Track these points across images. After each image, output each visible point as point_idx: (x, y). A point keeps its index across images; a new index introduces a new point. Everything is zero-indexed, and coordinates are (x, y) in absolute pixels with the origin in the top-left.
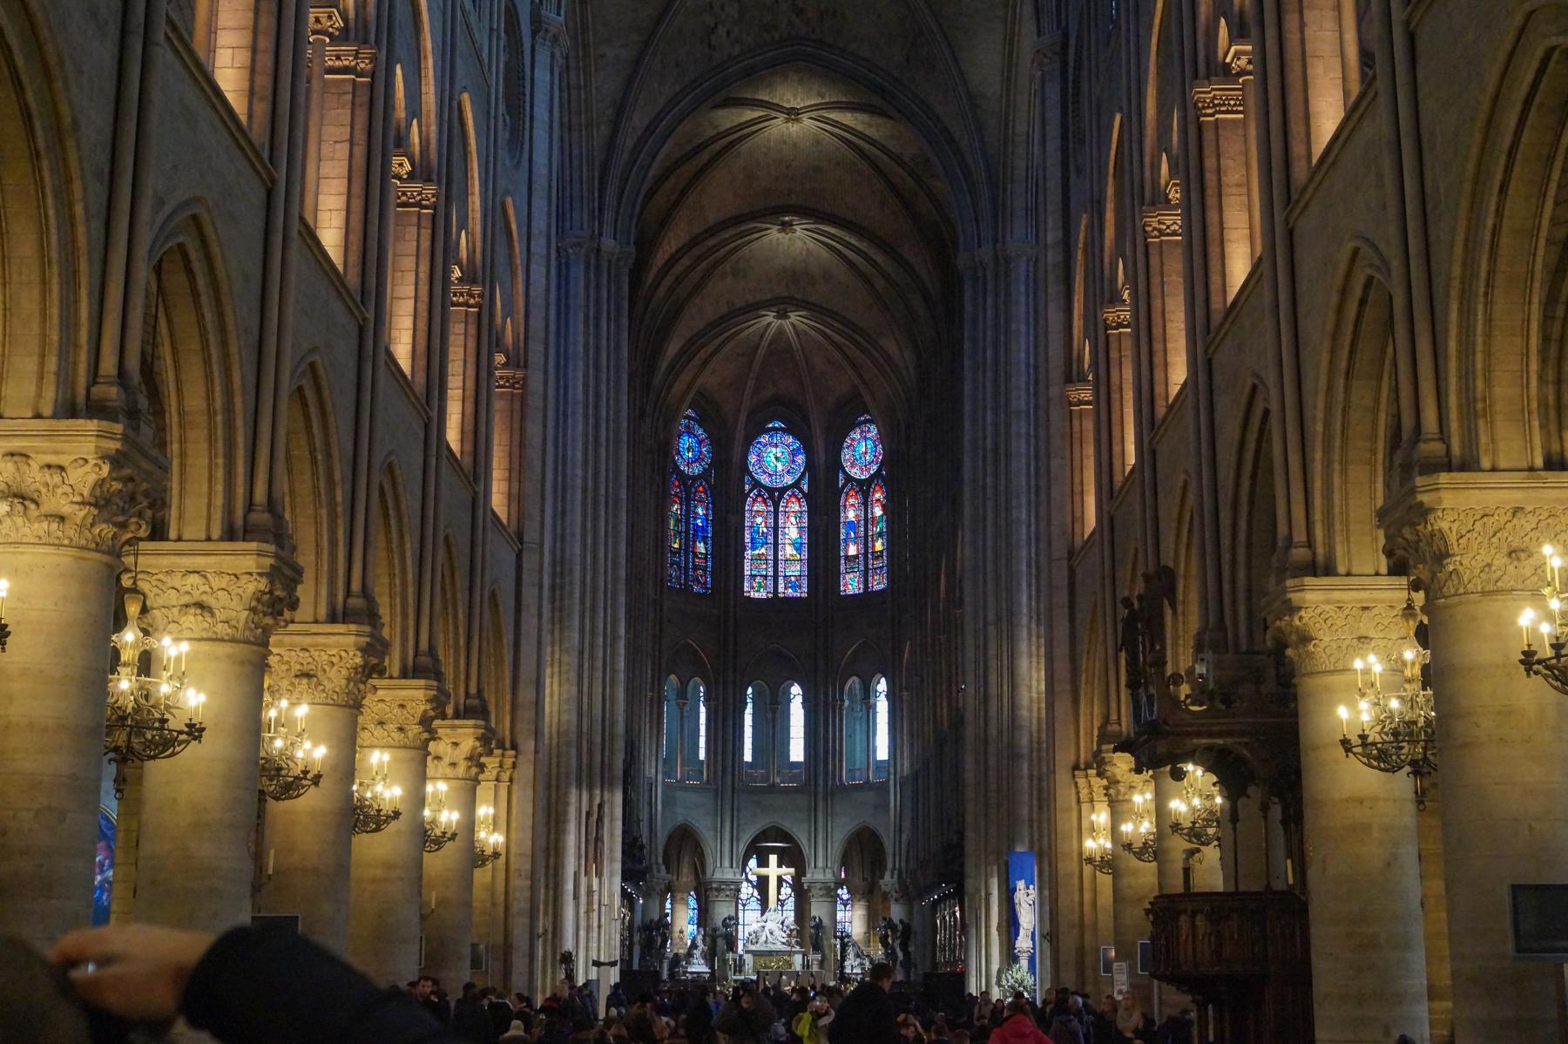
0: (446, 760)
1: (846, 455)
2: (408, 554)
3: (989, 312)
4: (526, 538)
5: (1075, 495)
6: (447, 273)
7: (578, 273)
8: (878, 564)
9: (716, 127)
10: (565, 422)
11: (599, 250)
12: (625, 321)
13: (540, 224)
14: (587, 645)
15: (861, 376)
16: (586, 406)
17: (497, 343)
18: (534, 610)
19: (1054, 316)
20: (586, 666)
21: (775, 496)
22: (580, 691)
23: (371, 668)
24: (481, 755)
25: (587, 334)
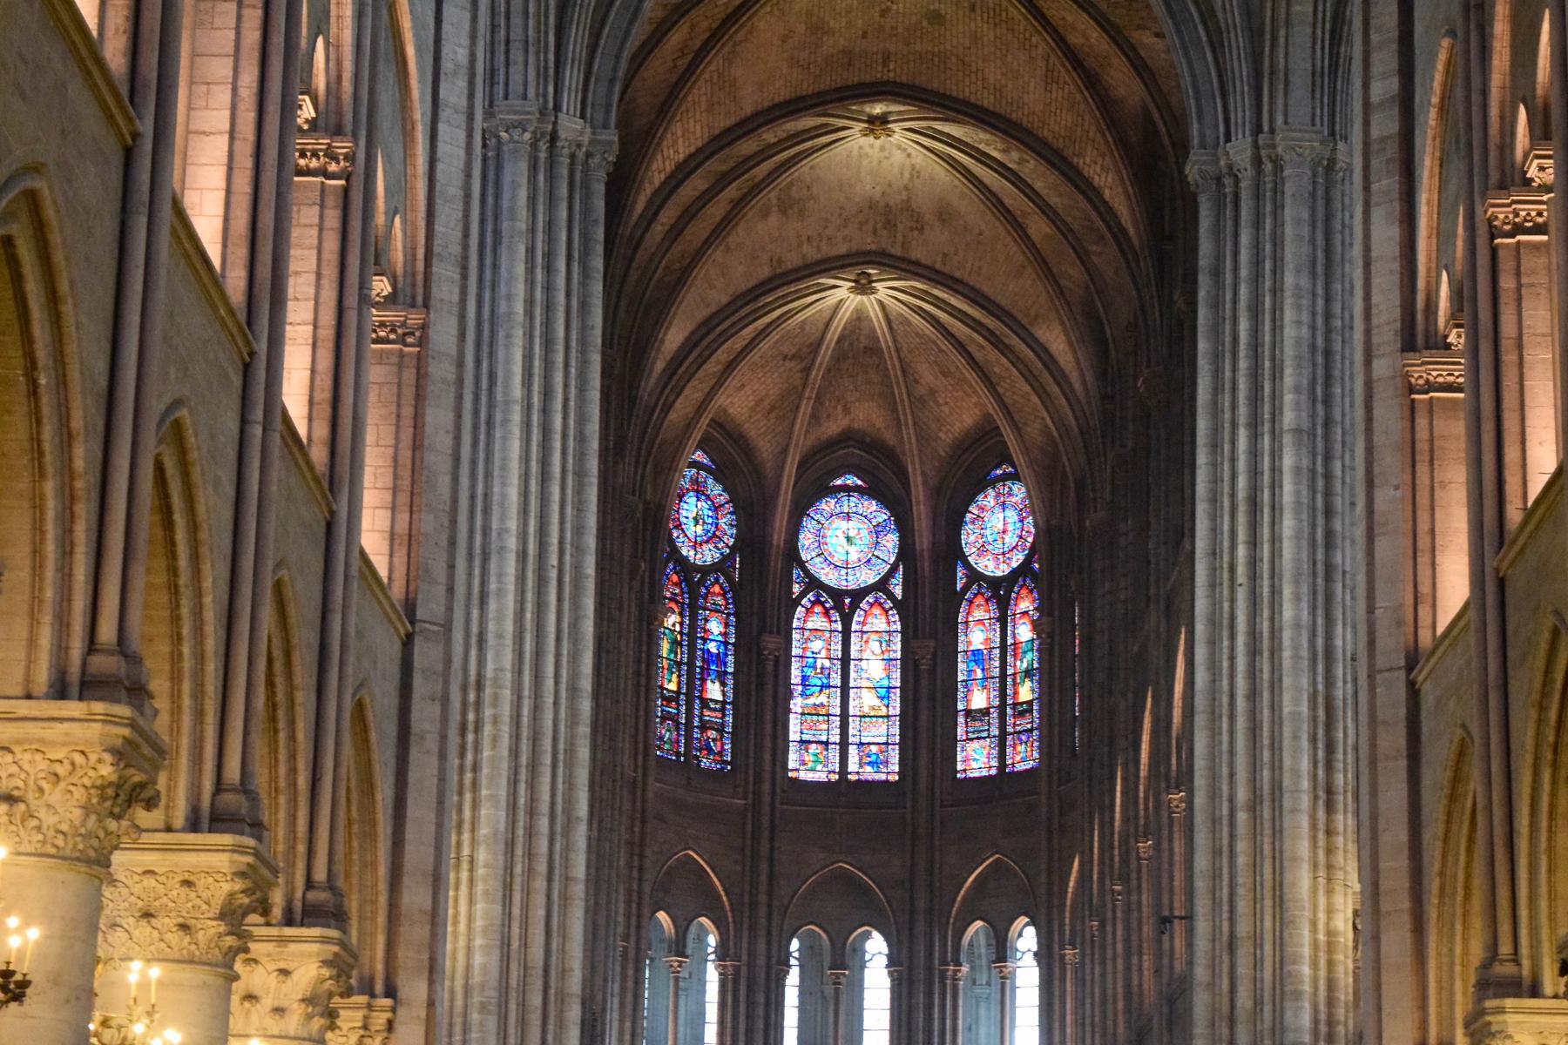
0: (267, 1003)
1: (969, 538)
2: (208, 600)
3: (1244, 256)
4: (420, 614)
5: (1420, 550)
6: (289, 108)
7: (516, 173)
8: (1024, 724)
10: (489, 434)
11: (554, 137)
12: (598, 263)
13: (456, 52)
14: (520, 832)
15: (999, 398)
16: (528, 408)
17: (376, 259)
18: (432, 743)
19: (1386, 234)
20: (518, 869)
21: (844, 603)
22: (507, 915)
23: (128, 795)
24: (331, 995)
25: (530, 282)
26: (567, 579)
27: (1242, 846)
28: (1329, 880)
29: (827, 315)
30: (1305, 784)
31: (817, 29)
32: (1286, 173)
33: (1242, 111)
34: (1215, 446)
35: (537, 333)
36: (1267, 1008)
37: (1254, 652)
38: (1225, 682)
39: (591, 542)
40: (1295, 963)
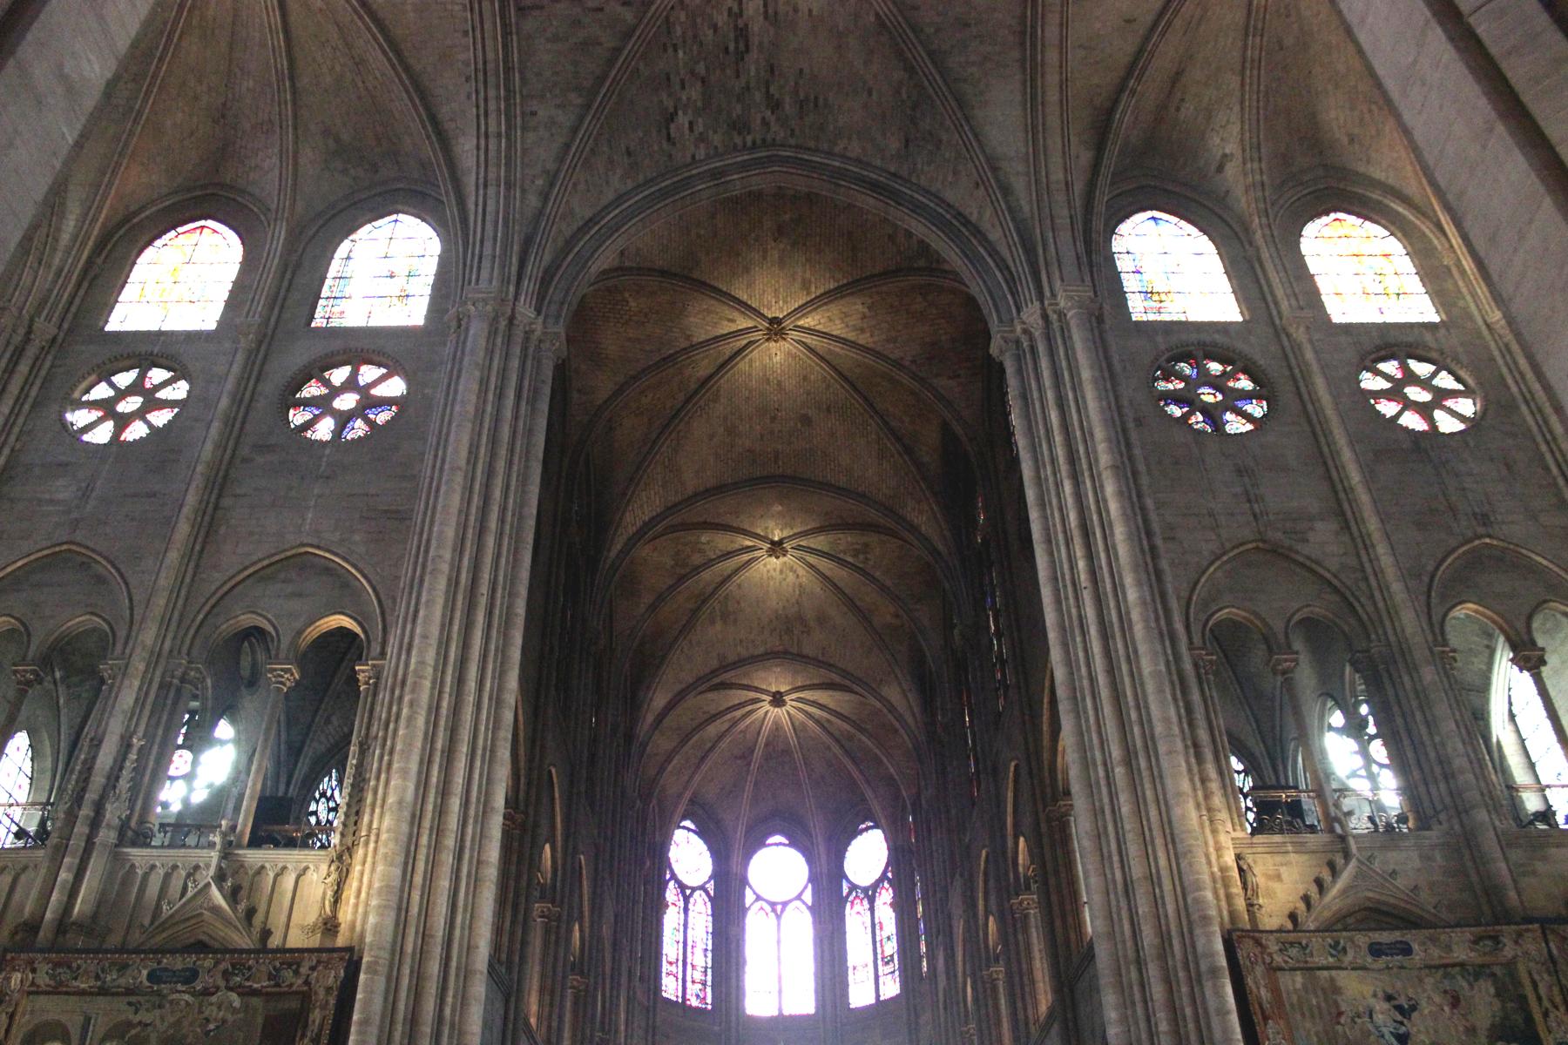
8: (889, 968)
9: (688, 337)
10: (436, 497)
12: (544, 406)
14: (430, 807)
20: (424, 840)
21: (777, 908)
26: (497, 612)
27: (1124, 799)
28: (1211, 821)
29: (757, 724)
30: (1176, 730)
31: (731, 431)
32: (1069, 315)
33: (1027, 289)
34: (1042, 505)
35: (485, 431)
36: (1176, 942)
37: (1105, 636)
38: (1084, 670)
39: (523, 590)
40: (1199, 889)
